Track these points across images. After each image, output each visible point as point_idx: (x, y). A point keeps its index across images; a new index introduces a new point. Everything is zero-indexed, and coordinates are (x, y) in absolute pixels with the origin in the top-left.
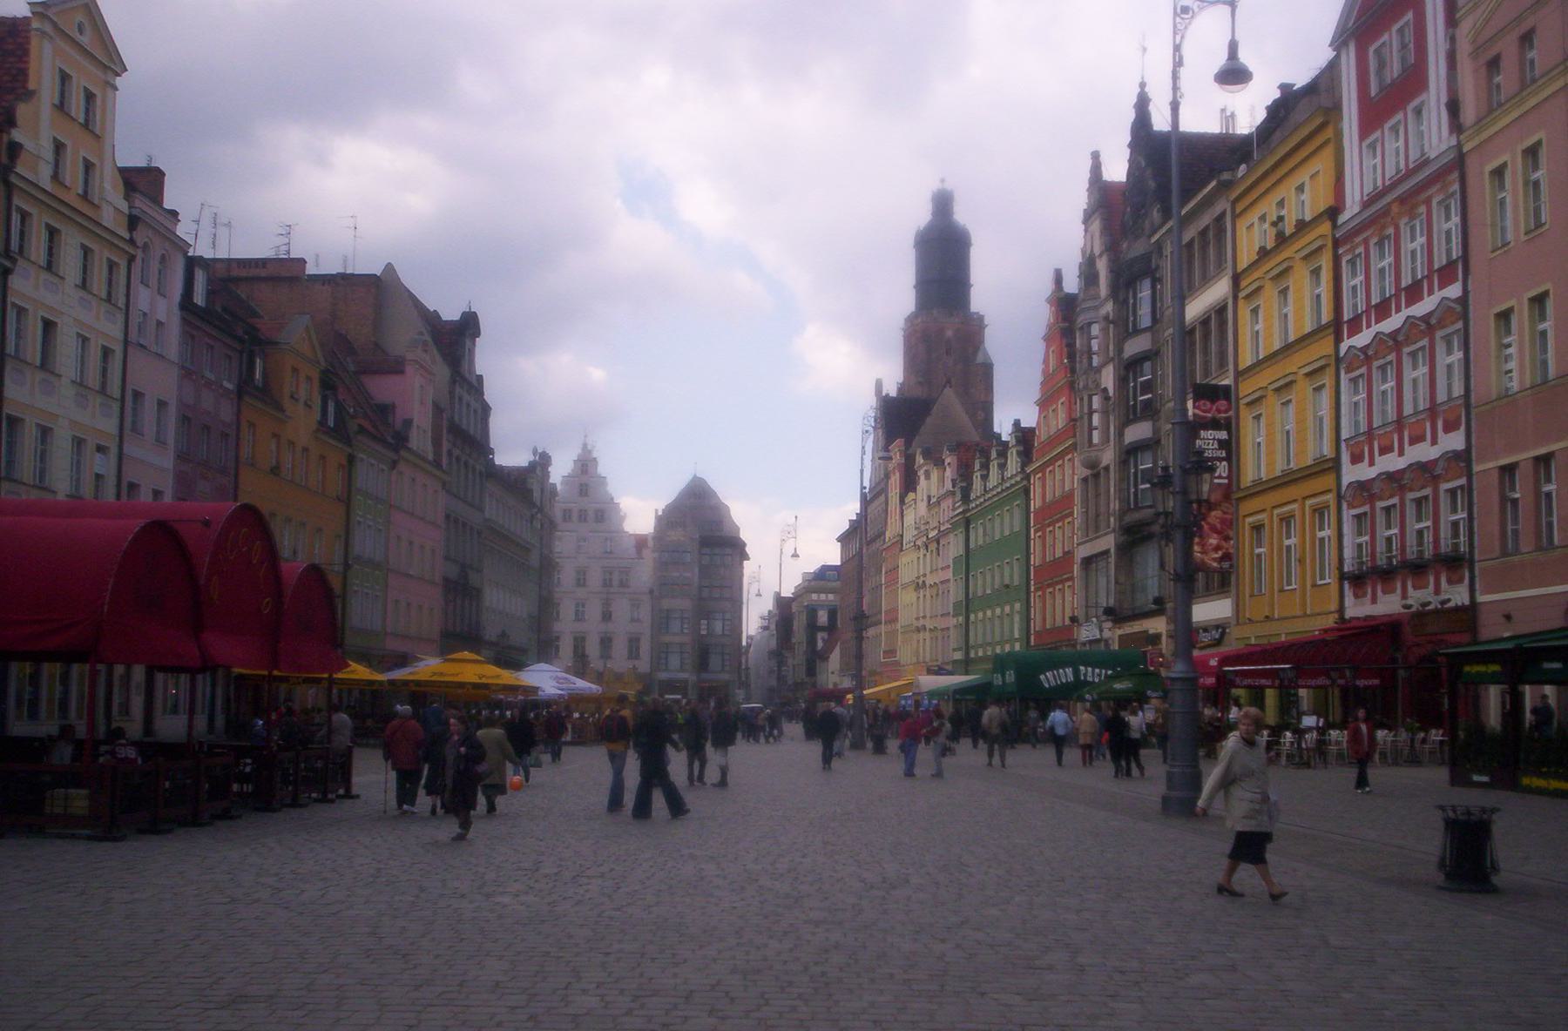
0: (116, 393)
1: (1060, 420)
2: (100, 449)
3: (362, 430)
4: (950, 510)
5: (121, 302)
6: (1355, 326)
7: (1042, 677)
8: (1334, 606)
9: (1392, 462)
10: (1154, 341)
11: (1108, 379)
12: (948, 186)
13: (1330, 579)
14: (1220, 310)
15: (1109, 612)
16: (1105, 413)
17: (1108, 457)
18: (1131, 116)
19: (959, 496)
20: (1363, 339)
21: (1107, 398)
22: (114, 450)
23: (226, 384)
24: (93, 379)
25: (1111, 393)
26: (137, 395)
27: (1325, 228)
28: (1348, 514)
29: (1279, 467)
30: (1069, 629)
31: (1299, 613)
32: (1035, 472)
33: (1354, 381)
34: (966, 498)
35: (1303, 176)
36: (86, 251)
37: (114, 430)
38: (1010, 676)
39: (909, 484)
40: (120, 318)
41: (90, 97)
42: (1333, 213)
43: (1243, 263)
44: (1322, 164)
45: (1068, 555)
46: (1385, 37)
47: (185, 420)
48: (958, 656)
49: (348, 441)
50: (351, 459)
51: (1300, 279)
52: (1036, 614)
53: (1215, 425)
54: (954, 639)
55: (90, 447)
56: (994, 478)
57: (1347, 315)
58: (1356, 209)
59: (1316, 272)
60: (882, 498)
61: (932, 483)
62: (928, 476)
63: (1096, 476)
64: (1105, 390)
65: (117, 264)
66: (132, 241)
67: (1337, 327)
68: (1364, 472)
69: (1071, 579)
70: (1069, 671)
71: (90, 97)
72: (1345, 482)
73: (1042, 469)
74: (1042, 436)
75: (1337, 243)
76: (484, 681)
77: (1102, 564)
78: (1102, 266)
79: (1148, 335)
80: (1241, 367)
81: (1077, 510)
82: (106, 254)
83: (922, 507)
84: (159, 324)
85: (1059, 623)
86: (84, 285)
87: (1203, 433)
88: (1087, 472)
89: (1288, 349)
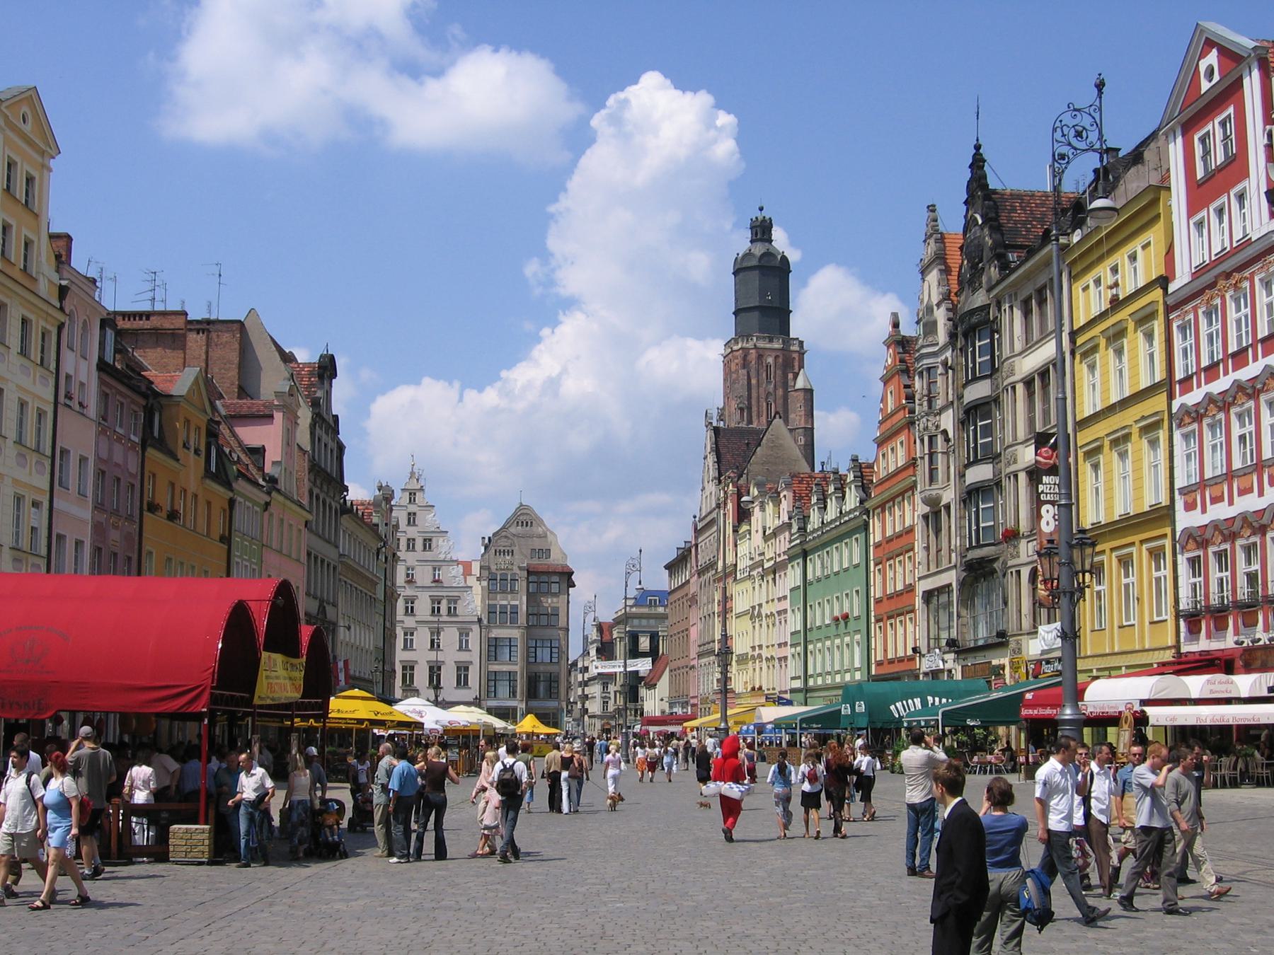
0: (48, 452)
1: (897, 457)
2: (36, 504)
3: (240, 474)
4: (783, 544)
5: (53, 366)
6: (1186, 384)
7: (892, 707)
8: (1170, 641)
9: (1221, 512)
10: (995, 387)
11: (947, 421)
12: (767, 214)
13: (1168, 615)
15: (952, 643)
17: (949, 496)
18: (967, 175)
20: (1194, 397)
21: (947, 440)
22: (46, 504)
23: (132, 437)
24: (30, 440)
25: (951, 435)
26: (64, 452)
27: (1157, 294)
28: (1182, 560)
29: (1118, 512)
30: (911, 659)
31: (1137, 648)
33: (1186, 437)
34: (802, 529)
35: (1136, 245)
36: (25, 321)
37: (46, 486)
38: (861, 707)
39: (743, 515)
40: (52, 382)
41: (30, 180)
43: (1080, 321)
44: (1154, 235)
45: (910, 589)
46: (1210, 127)
47: (101, 474)
48: (798, 684)
49: (228, 485)
50: (232, 502)
51: (1135, 341)
52: (877, 643)
53: (1053, 471)
54: (794, 667)
55: (27, 503)
56: (832, 513)
57: (1179, 375)
58: (1187, 279)
59: (1149, 336)
61: (765, 517)
62: (763, 509)
63: (937, 514)
64: (945, 432)
65: (50, 332)
66: (62, 309)
67: (1168, 386)
70: (918, 701)
71: (30, 180)
72: (1179, 529)
73: (882, 506)
74: (881, 471)
75: (1169, 309)
76: (379, 717)
77: (943, 598)
78: (941, 315)
79: (988, 381)
81: (919, 546)
82: (42, 323)
83: (757, 538)
84: (82, 384)
85: (901, 653)
86: (24, 352)
87: (1045, 479)
88: (927, 509)
89: (1124, 403)
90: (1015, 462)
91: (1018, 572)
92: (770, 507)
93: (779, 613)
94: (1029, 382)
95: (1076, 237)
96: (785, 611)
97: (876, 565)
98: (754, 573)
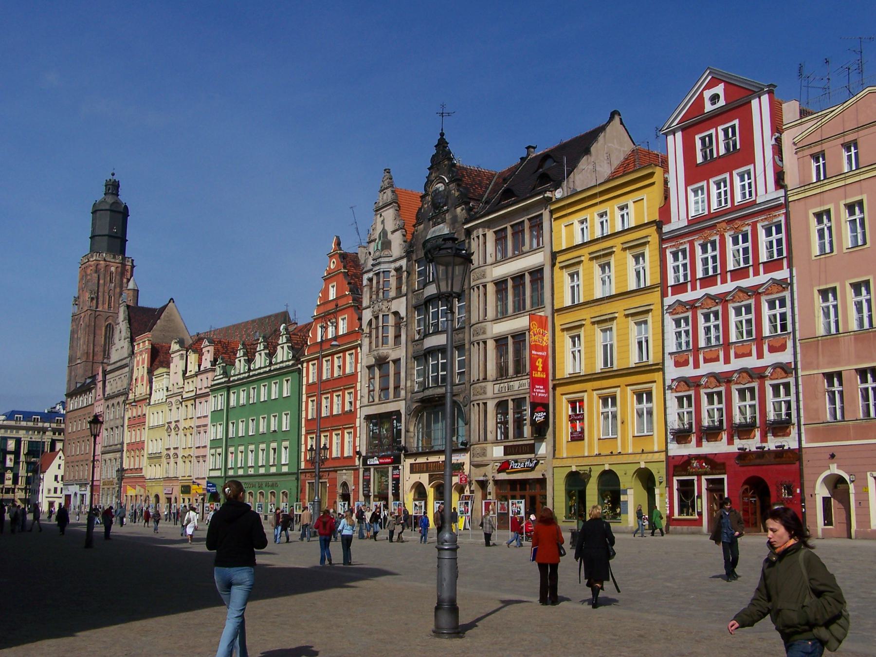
4: (204, 382)
9: (719, 367)
14: (537, 274)
16: (398, 326)
19: (219, 370)
25: (403, 314)
32: (308, 361)
35: (629, 200)
42: (659, 225)
46: (713, 131)
56: (260, 360)
57: (671, 281)
60: (127, 369)
68: (689, 371)
69: (355, 428)
80: (555, 308)
90: (484, 333)
91: (485, 404)
92: (193, 357)
93: (198, 427)
94: (500, 284)
95: (558, 194)
96: (206, 426)
97: (308, 397)
98: (173, 400)
